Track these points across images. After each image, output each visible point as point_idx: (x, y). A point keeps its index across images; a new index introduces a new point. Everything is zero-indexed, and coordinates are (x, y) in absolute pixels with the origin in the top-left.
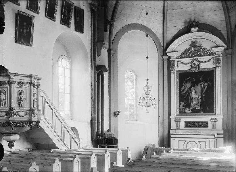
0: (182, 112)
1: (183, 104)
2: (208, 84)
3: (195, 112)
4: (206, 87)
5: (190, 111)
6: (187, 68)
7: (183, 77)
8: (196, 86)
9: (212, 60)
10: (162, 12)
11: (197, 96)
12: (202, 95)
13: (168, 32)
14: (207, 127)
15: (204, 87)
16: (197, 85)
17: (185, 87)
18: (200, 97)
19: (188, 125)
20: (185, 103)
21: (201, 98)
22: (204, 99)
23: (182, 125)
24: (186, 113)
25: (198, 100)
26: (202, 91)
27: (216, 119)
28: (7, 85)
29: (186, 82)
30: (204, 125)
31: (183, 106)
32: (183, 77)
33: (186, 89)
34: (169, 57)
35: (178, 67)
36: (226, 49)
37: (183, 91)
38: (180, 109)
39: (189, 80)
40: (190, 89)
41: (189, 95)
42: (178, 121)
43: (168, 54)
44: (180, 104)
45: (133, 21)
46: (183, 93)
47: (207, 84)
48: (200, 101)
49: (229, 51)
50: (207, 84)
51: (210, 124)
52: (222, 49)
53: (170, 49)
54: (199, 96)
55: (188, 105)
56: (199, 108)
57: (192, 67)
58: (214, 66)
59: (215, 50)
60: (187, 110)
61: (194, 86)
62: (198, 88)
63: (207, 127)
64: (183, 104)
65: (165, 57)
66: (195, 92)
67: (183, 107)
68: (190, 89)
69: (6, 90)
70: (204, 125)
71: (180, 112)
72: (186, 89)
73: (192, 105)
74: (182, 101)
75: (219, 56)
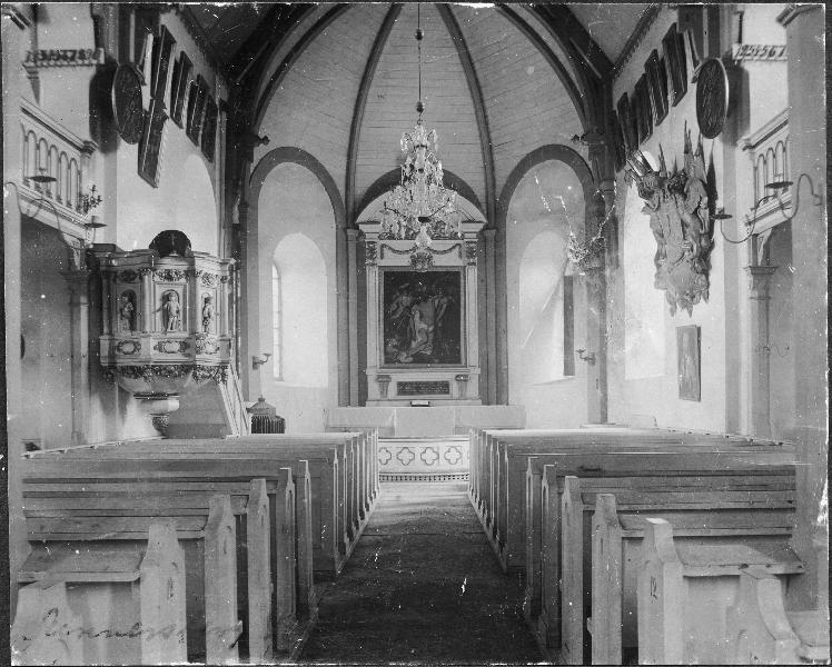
0: (390, 360)
1: (394, 342)
2: (449, 301)
3: (420, 360)
4: (445, 306)
5: (411, 359)
6: (403, 261)
7: (395, 281)
8: (422, 304)
9: (457, 249)
10: (349, 129)
11: (424, 326)
12: (435, 324)
13: (358, 175)
14: (448, 393)
15: (440, 306)
16: (425, 301)
17: (397, 304)
18: (431, 329)
19: (404, 388)
20: (398, 341)
21: (434, 331)
22: (439, 332)
23: (393, 389)
24: (400, 362)
25: (427, 333)
26: (436, 315)
27: (466, 376)
28: (183, 280)
29: (402, 293)
30: (443, 388)
31: (394, 347)
32: (395, 281)
33: (402, 308)
34: (361, 234)
35: (382, 258)
36: (487, 228)
37: (394, 312)
38: (386, 353)
39: (406, 288)
40: (409, 308)
41: (407, 323)
42: (383, 381)
43: (361, 227)
44: (386, 344)
45: (290, 142)
46: (394, 317)
47: (445, 300)
48: (431, 335)
49: (491, 234)
50: (445, 300)
51: (454, 387)
52: (481, 226)
53: (362, 217)
54: (429, 326)
55: (405, 344)
56: (429, 353)
57: (414, 261)
58: (460, 263)
59: (460, 229)
60: (403, 357)
61: (418, 303)
62: (428, 309)
63: (448, 393)
64: (394, 342)
65: (351, 232)
66: (421, 317)
67: (395, 350)
68: (409, 308)
69: (180, 290)
70: (443, 388)
71: (386, 362)
72: (402, 308)
73: (414, 344)
74: (392, 336)
75: (472, 242)
